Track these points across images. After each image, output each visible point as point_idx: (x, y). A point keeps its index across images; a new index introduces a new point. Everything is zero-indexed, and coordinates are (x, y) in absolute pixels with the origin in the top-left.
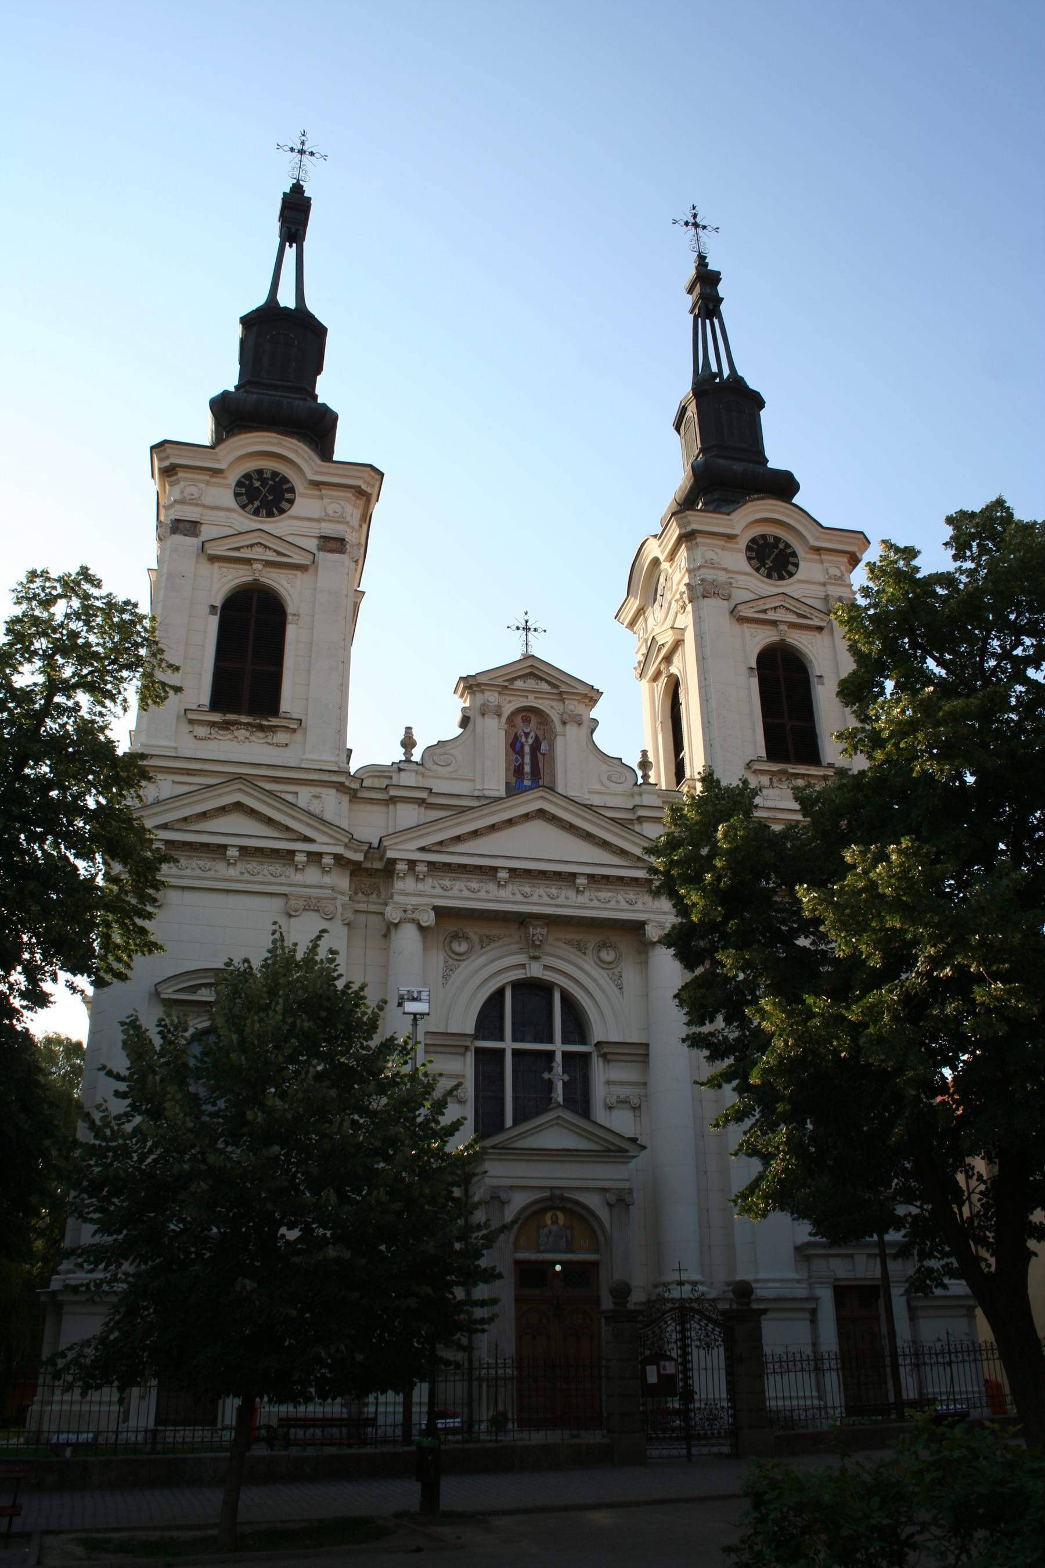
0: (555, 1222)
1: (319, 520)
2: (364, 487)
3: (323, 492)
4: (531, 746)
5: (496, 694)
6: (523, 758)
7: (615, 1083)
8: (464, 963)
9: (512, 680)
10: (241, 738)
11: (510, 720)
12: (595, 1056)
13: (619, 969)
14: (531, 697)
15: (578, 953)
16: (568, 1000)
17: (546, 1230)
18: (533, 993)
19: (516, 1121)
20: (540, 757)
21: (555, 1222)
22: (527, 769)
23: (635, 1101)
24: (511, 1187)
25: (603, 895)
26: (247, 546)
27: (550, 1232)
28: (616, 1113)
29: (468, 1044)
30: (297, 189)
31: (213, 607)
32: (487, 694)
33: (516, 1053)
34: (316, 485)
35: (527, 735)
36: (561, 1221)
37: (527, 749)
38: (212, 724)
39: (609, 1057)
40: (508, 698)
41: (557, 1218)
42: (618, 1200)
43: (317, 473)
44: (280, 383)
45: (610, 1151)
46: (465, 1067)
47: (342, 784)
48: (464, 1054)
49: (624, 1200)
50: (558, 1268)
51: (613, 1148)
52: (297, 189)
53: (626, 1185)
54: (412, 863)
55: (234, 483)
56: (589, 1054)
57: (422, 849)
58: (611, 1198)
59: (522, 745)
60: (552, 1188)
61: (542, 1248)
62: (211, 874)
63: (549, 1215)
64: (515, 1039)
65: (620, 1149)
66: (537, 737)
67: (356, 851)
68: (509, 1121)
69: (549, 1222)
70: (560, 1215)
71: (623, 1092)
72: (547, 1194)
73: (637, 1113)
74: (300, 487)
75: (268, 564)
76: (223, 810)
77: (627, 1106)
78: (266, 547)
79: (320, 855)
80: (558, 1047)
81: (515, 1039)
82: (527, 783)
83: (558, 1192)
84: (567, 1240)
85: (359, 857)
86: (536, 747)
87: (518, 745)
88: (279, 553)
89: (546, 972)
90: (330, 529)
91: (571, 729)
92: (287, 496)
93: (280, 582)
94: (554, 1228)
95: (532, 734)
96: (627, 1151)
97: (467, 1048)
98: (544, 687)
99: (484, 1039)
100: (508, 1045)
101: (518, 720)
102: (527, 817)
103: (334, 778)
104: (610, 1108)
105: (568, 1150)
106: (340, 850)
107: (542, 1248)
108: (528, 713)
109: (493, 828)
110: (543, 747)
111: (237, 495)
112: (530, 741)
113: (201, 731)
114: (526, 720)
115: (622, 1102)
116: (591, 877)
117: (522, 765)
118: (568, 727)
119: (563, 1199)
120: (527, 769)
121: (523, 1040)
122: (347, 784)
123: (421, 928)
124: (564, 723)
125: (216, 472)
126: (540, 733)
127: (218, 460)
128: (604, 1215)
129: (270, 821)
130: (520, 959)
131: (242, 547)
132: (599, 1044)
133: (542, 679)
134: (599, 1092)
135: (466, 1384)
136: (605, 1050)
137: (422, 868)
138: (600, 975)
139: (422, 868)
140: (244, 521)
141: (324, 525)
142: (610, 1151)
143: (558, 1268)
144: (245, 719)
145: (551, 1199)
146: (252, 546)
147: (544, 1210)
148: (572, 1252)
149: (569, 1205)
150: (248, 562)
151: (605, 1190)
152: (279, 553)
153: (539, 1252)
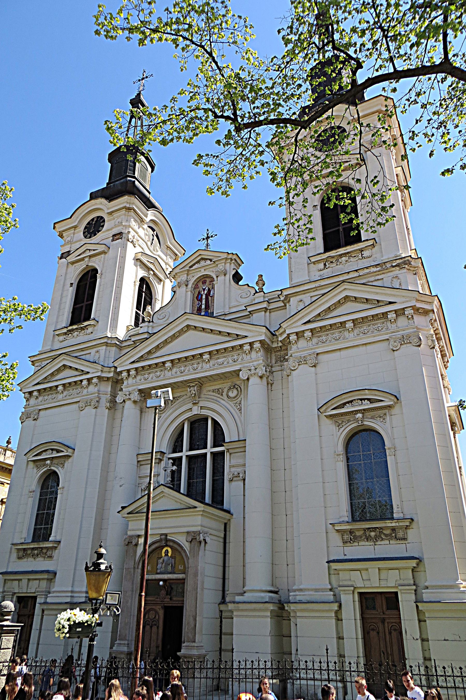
0: (166, 555)
2: (128, 206)
4: (206, 294)
5: (186, 275)
6: (201, 302)
8: (163, 415)
9: (190, 267)
10: (75, 336)
11: (196, 286)
13: (240, 399)
14: (202, 270)
15: (219, 396)
16: (215, 423)
17: (161, 560)
18: (197, 424)
20: (210, 298)
21: (166, 555)
22: (203, 306)
25: (220, 361)
27: (163, 561)
31: (72, 284)
32: (181, 277)
34: (110, 213)
35: (204, 290)
36: (169, 555)
37: (204, 297)
38: (65, 334)
40: (193, 275)
41: (168, 552)
43: (108, 209)
47: (106, 342)
50: (161, 583)
54: (128, 371)
57: (133, 362)
59: (202, 295)
62: (55, 400)
66: (209, 289)
67: (109, 372)
69: (163, 555)
70: (169, 550)
75: (90, 257)
78: (90, 250)
79: (92, 378)
82: (203, 313)
85: (111, 375)
86: (208, 295)
87: (200, 296)
88: (94, 250)
89: (202, 411)
90: (115, 231)
91: (221, 278)
92: (102, 224)
94: (166, 558)
95: (207, 288)
96: (196, 507)
98: (208, 262)
101: (201, 283)
102: (181, 332)
103: (102, 341)
106: (99, 374)
107: (158, 571)
108: (204, 279)
109: (166, 342)
110: (211, 293)
112: (206, 292)
113: (61, 338)
114: (204, 283)
116: (210, 353)
117: (201, 306)
118: (219, 278)
119: (167, 540)
120: (203, 306)
122: (109, 342)
123: (135, 402)
124: (217, 277)
125: (75, 227)
126: (210, 287)
129: (77, 369)
130: (190, 405)
133: (207, 259)
137: (133, 372)
138: (230, 405)
139: (133, 372)
141: (113, 230)
144: (75, 327)
145: (160, 540)
146: (85, 252)
148: (174, 573)
149: (171, 544)
150: (83, 259)
152: (94, 250)
153: (157, 573)
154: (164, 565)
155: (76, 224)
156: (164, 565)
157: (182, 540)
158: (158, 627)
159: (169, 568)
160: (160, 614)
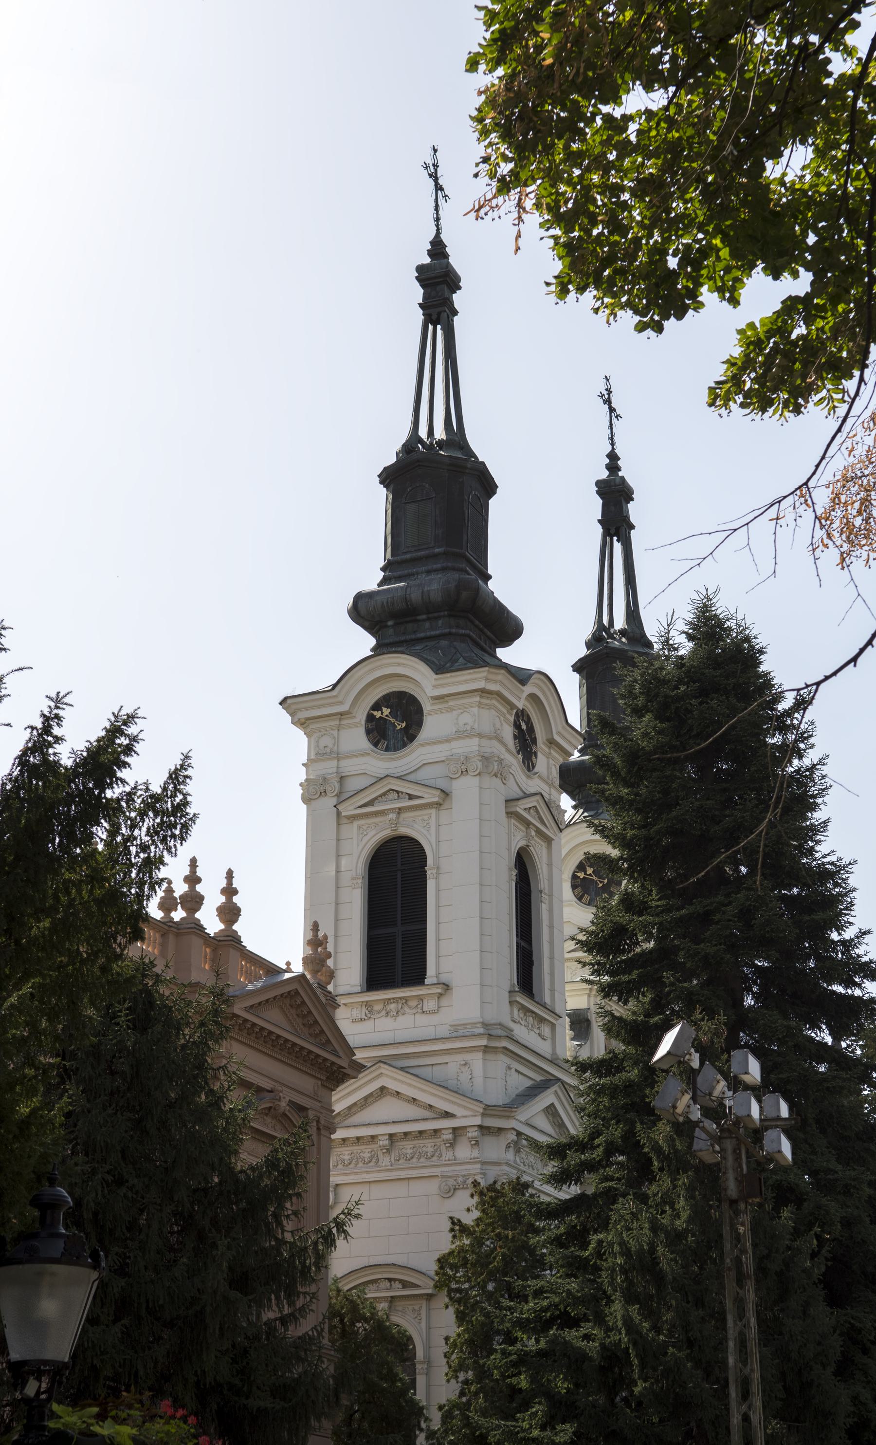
1: (448, 740)
3: (451, 703)
26: (381, 796)
30: (438, 249)
43: (435, 687)
44: (420, 554)
52: (438, 249)
55: (363, 722)
74: (427, 707)
76: (367, 1101)
93: (415, 827)
111: (368, 732)
127: (341, 703)
131: (376, 798)
140: (378, 763)
141: (454, 744)
146: (384, 794)
155: (345, 708)
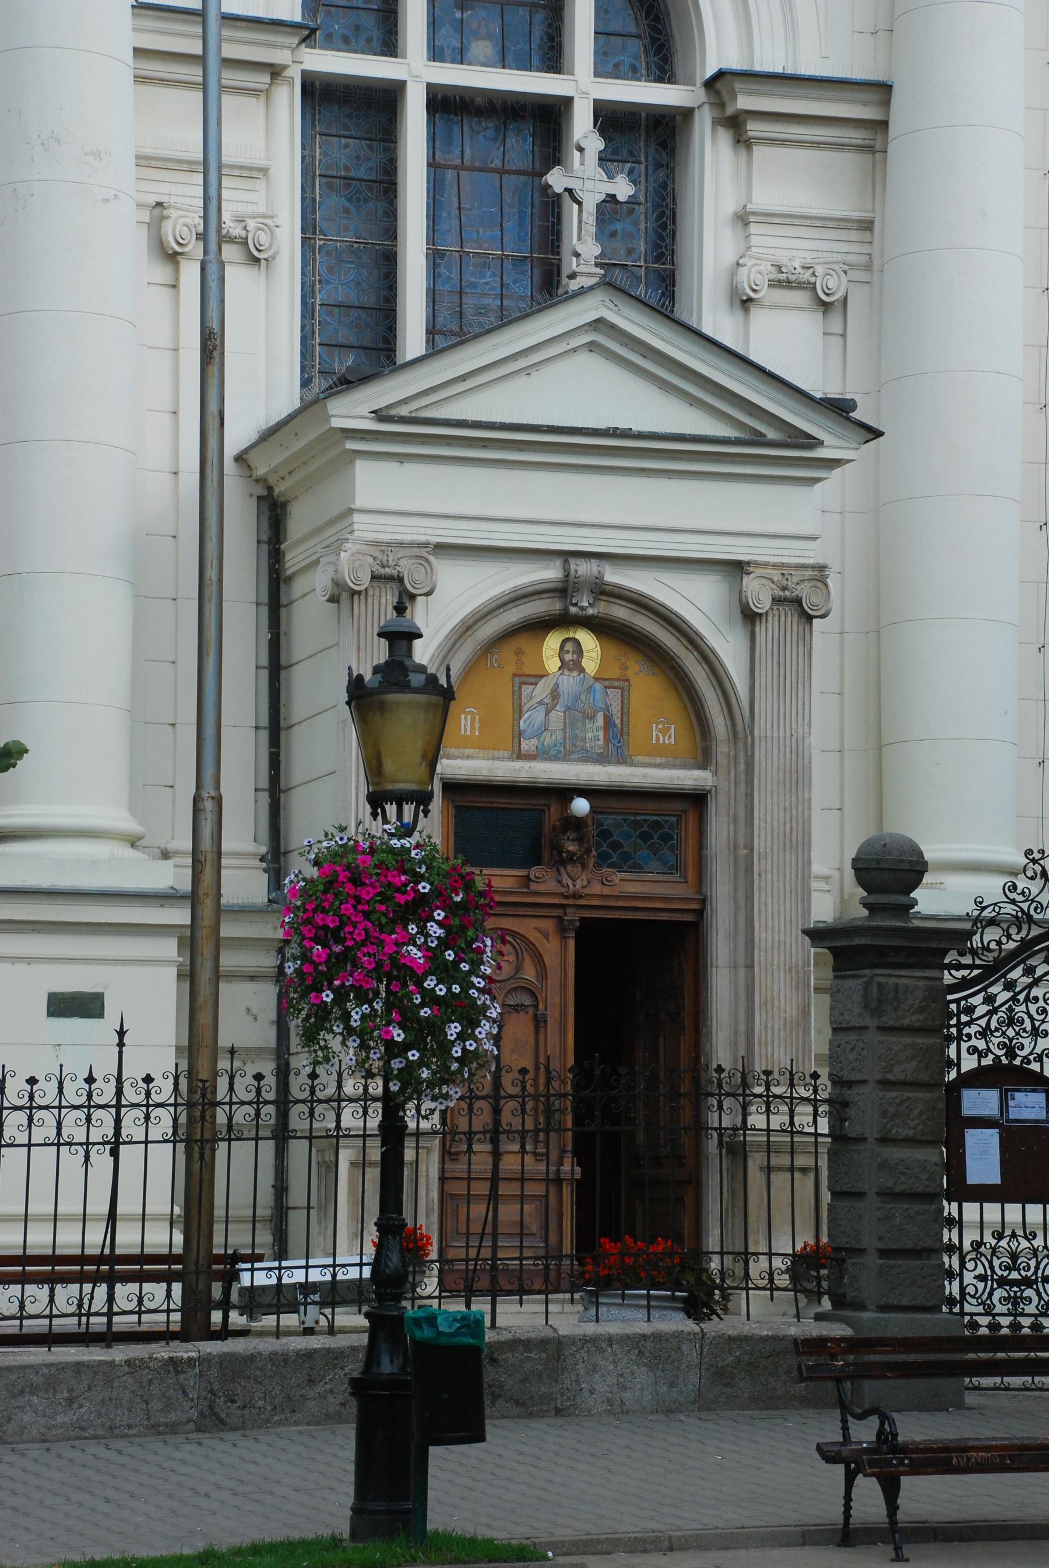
0: (572, 662)
7: (769, 217)
12: (704, 122)
17: (541, 691)
19: (444, 336)
21: (572, 662)
23: (835, 285)
24: (442, 549)
27: (555, 694)
28: (759, 317)
29: (279, 56)
33: (444, 104)
39: (754, 128)
42: (777, 601)
45: (758, 440)
46: (269, 136)
48: (265, 94)
49: (798, 601)
51: (771, 434)
53: (809, 554)
56: (687, 113)
58: (759, 592)
60: (567, 556)
61: (526, 745)
63: (553, 642)
64: (436, 54)
65: (779, 435)
68: (413, 338)
69: (552, 664)
70: (587, 639)
71: (796, 250)
72: (550, 573)
73: (835, 323)
77: (800, 297)
80: (583, 84)
81: (436, 54)
83: (584, 569)
84: (608, 721)
94: (569, 683)
97: (275, 71)
99: (331, 43)
100: (415, 69)
104: (746, 303)
105: (626, 434)
115: (787, 284)
119: (603, 591)
121: (460, 57)
128: (728, 647)
132: (718, 83)
134: (713, 249)
135: (268, 1148)
136: (744, 102)
142: (758, 440)
143: (581, 806)
145: (564, 590)
147: (541, 626)
148: (622, 760)
149: (620, 612)
151: (738, 568)
153: (520, 756)
154: (557, 715)
156: (557, 715)
157: (696, 601)
158: (539, 1022)
159: (594, 733)
160: (551, 958)
